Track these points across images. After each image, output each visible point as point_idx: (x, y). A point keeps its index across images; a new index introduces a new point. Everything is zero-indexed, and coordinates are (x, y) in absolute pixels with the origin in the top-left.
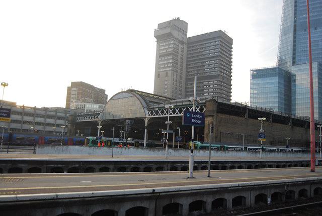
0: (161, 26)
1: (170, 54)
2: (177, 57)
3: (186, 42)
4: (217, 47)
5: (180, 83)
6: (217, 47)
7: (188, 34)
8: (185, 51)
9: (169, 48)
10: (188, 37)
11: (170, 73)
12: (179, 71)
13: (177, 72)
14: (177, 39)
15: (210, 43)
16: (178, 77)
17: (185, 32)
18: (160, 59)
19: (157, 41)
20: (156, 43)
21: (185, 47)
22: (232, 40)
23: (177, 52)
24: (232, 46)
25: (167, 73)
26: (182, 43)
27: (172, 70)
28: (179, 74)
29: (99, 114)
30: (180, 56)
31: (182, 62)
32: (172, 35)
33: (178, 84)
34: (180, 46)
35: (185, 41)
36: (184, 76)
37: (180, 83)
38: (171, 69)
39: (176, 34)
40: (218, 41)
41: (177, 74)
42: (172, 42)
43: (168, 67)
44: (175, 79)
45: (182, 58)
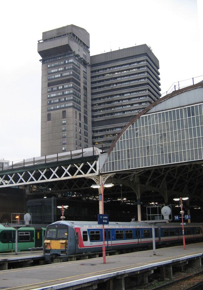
0: (48, 37)
1: (68, 81)
2: (79, 84)
3: (90, 64)
4: (142, 70)
5: (86, 128)
6: (142, 70)
7: (91, 50)
8: (89, 75)
9: (65, 70)
10: (92, 54)
11: (70, 112)
12: (82, 109)
13: (80, 110)
14: (78, 56)
15: (130, 64)
16: (83, 119)
17: (86, 47)
18: (49, 90)
19: (43, 61)
20: (41, 63)
21: (89, 70)
22: (158, 61)
23: (78, 78)
24: (159, 71)
25: (64, 112)
26: (85, 64)
27: (73, 107)
28: (83, 114)
29: (94, 158)
30: (82, 85)
31: (85, 95)
32: (71, 50)
33: (83, 131)
34: (82, 68)
35: (88, 61)
36: (90, 119)
37: (86, 128)
38: (71, 104)
39: (75, 47)
40: (143, 61)
41: (80, 114)
42: (71, 61)
43: (65, 101)
44: (78, 122)
45: (85, 89)
